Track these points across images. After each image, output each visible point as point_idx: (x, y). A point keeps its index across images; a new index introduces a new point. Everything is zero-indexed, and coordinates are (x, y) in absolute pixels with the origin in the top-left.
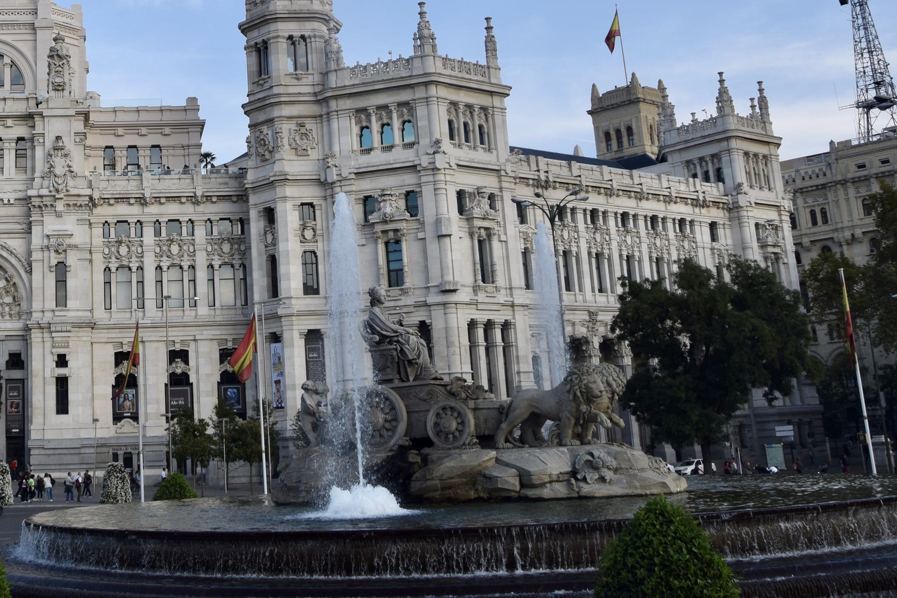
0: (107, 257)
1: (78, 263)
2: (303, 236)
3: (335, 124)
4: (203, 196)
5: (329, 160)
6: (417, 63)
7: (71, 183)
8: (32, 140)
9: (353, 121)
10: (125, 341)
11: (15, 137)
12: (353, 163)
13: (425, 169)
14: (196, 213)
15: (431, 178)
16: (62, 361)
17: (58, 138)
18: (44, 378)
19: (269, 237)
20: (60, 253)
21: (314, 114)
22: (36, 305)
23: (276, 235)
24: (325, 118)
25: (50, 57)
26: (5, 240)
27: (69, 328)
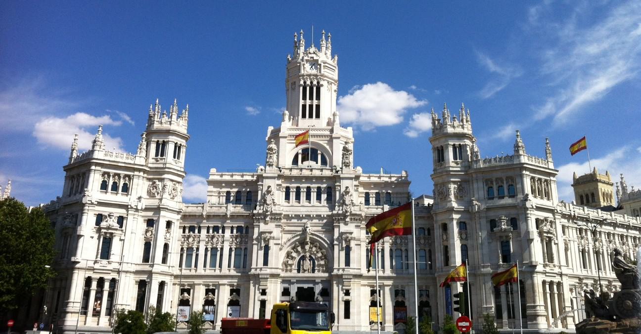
1: (356, 246)
3: (475, 186)
5: (474, 202)
7: (352, 208)
9: (485, 184)
13: (521, 208)
17: (347, 188)
19: (445, 237)
20: (348, 242)
22: (336, 266)
23: (448, 236)
27: (351, 277)
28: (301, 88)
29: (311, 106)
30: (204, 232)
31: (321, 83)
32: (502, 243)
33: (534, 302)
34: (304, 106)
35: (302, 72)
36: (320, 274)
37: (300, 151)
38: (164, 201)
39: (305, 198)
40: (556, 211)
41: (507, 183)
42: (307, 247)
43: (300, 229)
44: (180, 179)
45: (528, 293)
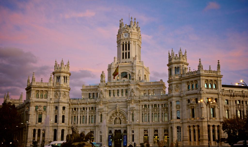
0: (142, 112)
2: (177, 107)
4: (161, 99)
6: (198, 72)
7: (135, 98)
8: (128, 90)
10: (146, 128)
11: (125, 89)
12: (186, 93)
13: (199, 94)
14: (160, 103)
15: (200, 96)
16: (133, 132)
18: (130, 135)
21: (179, 83)
24: (180, 83)
25: (132, 73)
26: (124, 109)
28: (122, 45)
29: (126, 53)
30: (79, 110)
31: (130, 42)
32: (192, 109)
33: (202, 134)
34: (123, 53)
35: (122, 38)
36: (123, 125)
37: (120, 74)
38: (60, 100)
39: (117, 95)
40: (219, 94)
41: (195, 83)
42: (118, 114)
43: (114, 107)
44: (68, 91)
45: (201, 131)
